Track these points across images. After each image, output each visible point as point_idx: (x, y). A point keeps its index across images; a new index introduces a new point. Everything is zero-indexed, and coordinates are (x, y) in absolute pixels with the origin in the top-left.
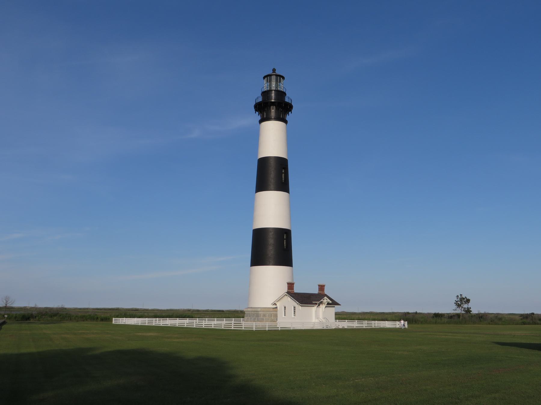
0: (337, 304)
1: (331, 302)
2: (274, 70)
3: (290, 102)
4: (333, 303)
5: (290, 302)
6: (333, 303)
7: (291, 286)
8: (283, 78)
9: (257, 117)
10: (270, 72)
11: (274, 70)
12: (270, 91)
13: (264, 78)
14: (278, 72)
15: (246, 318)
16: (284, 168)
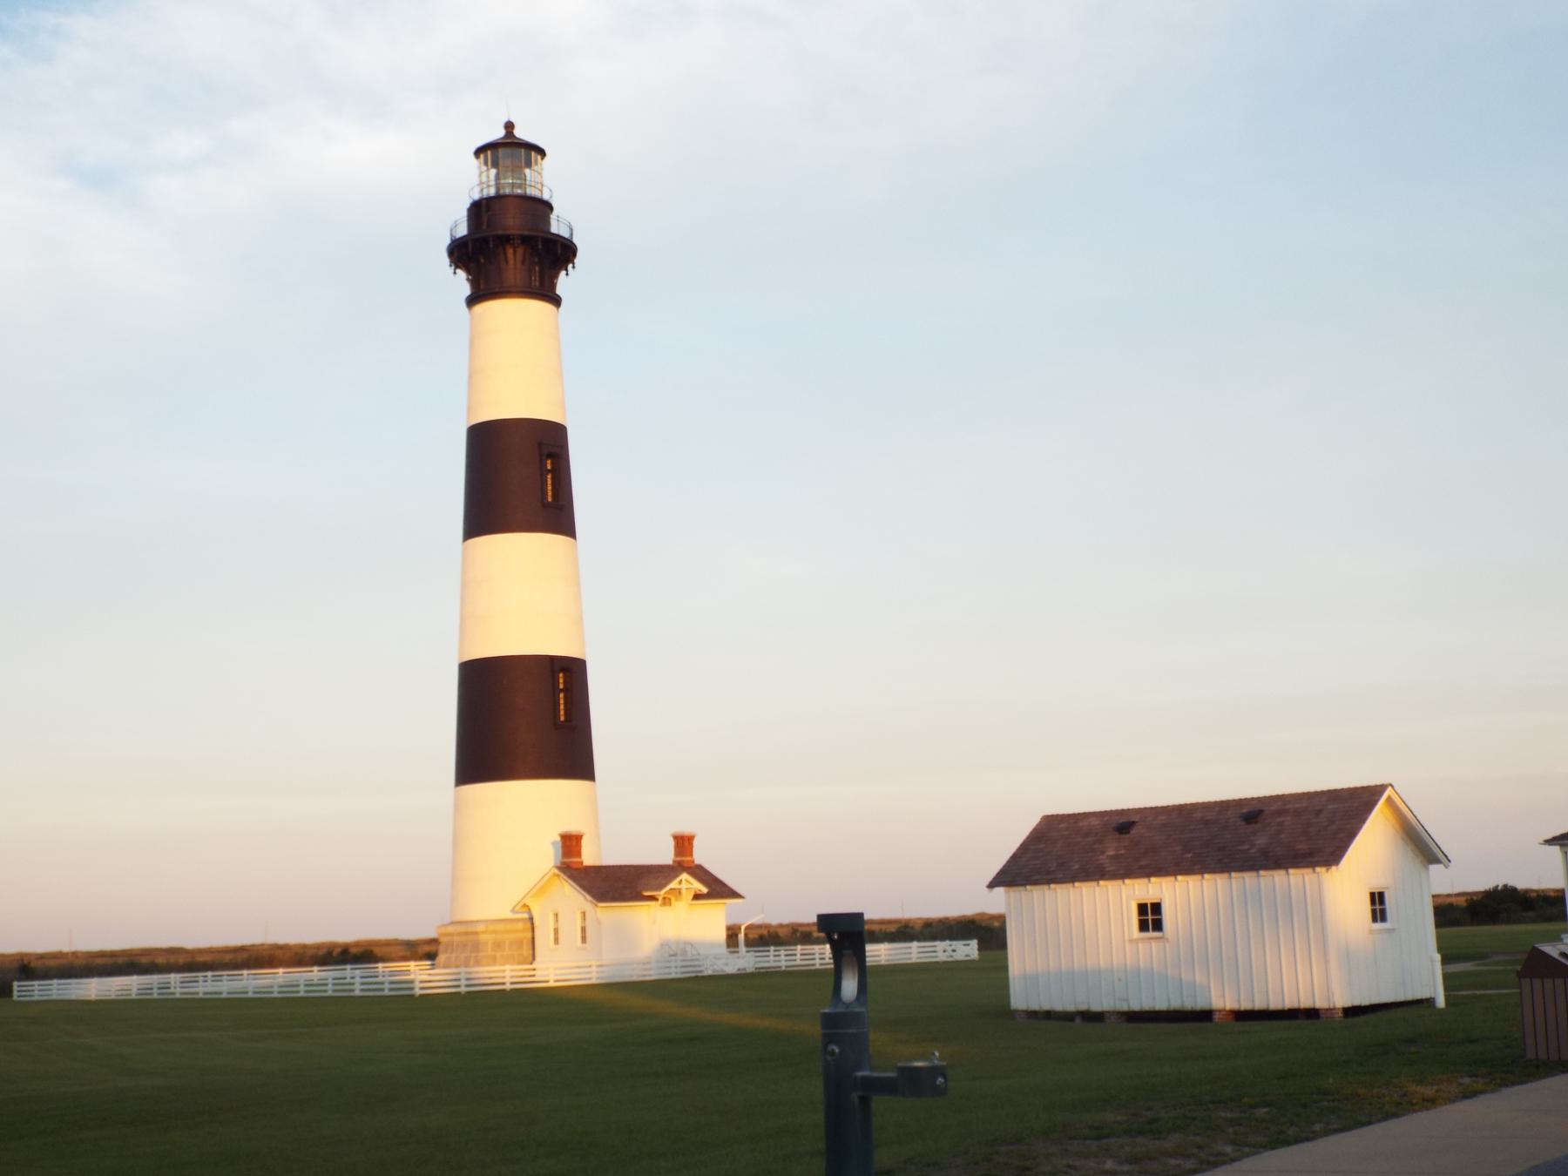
0: (734, 894)
1: (705, 890)
2: (509, 126)
3: (566, 234)
4: (717, 889)
5: (571, 898)
6: (717, 889)
7: (570, 843)
8: (541, 152)
9: (460, 284)
10: (498, 133)
11: (509, 126)
12: (499, 197)
13: (479, 152)
14: (520, 133)
15: (441, 958)
16: (550, 456)
